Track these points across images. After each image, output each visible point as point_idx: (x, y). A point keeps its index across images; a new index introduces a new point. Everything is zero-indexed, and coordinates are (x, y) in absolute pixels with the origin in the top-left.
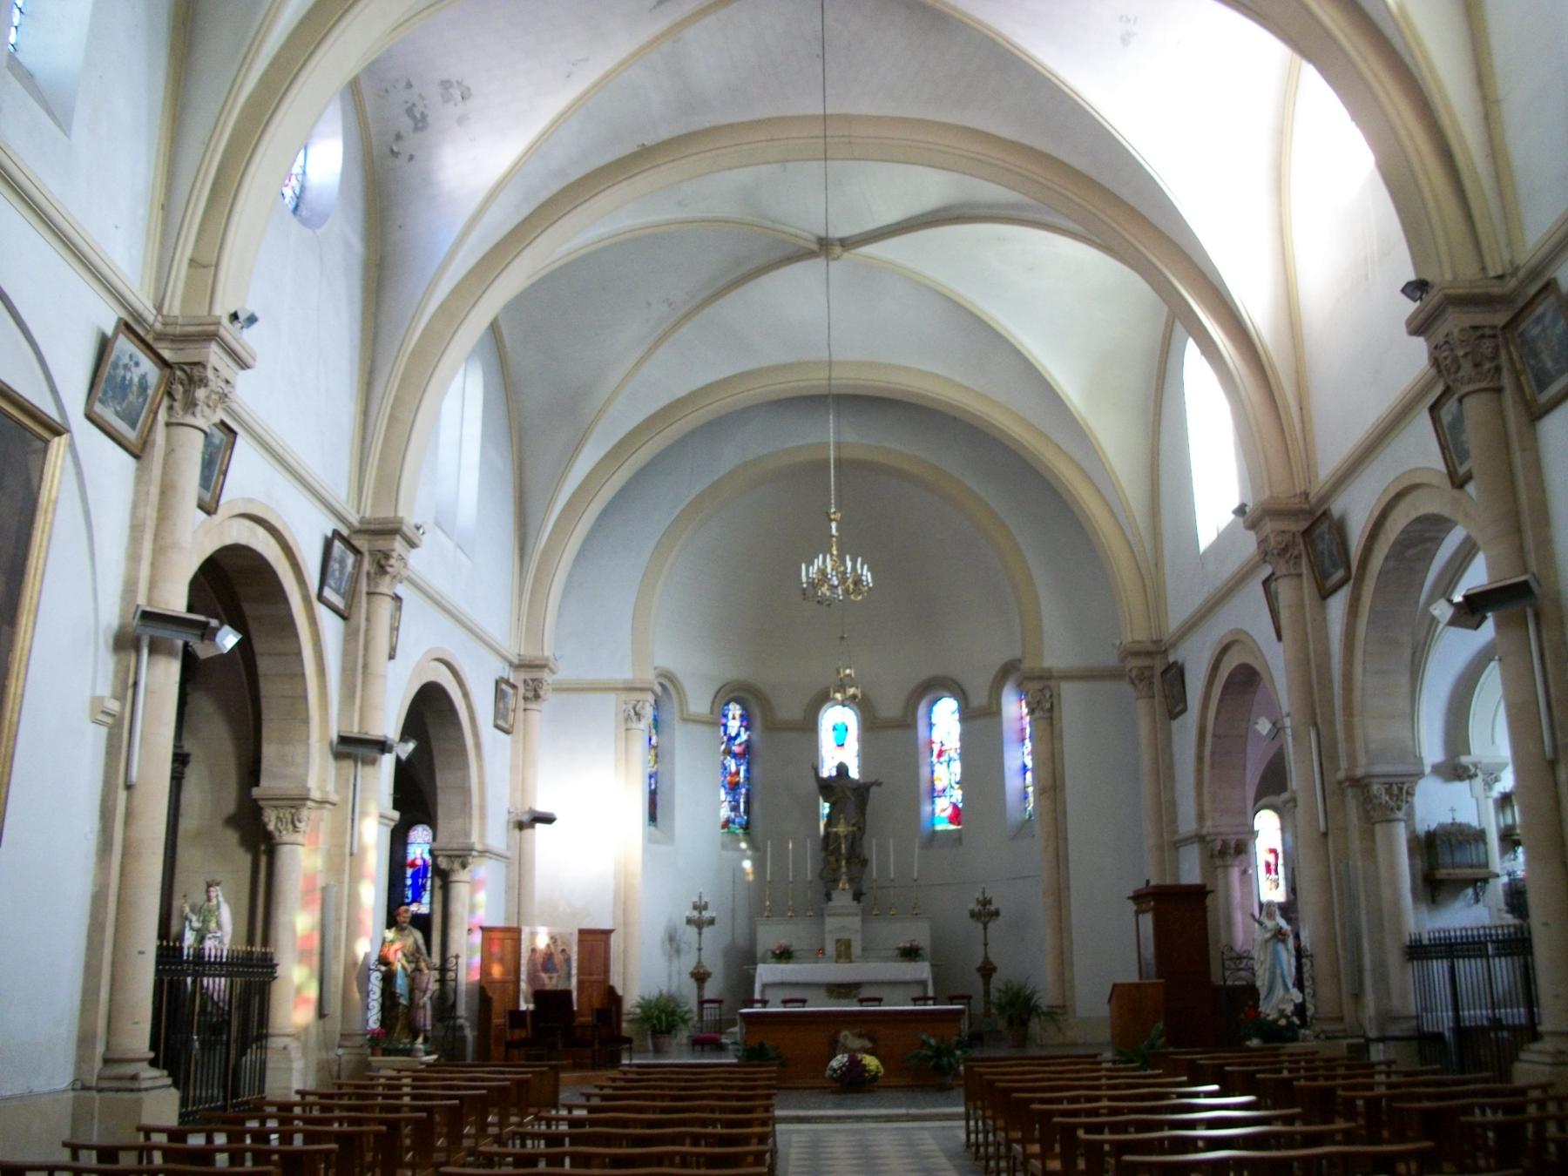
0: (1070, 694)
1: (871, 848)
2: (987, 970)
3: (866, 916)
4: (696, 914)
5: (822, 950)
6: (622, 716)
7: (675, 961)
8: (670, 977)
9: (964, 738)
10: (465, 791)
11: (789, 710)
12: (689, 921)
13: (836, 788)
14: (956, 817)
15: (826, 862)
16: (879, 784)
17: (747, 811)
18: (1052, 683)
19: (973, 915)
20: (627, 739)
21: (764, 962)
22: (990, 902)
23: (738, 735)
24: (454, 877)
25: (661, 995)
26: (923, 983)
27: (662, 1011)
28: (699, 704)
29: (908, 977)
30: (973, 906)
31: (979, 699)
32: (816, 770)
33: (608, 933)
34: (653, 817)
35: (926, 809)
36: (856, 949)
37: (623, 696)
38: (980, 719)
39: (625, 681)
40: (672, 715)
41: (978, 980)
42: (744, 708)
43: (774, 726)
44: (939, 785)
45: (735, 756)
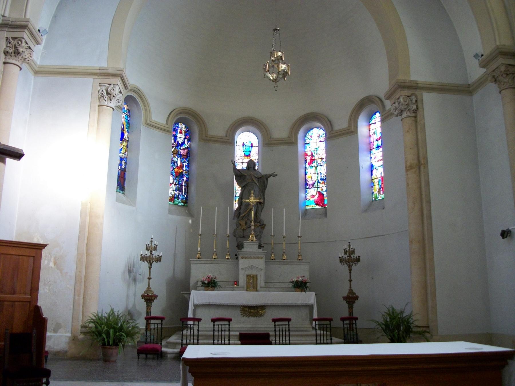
0: (428, 99)
1: (270, 216)
2: (351, 299)
3: (269, 260)
4: (148, 253)
5: (236, 283)
6: (96, 95)
7: (132, 287)
8: (128, 297)
9: (328, 150)
11: (217, 130)
12: (143, 258)
13: (248, 177)
14: (320, 200)
15: (238, 225)
16: (275, 176)
17: (187, 192)
18: (417, 92)
19: (341, 260)
20: (99, 112)
21: (196, 289)
22: (353, 252)
23: (183, 143)
25: (112, 313)
26: (310, 307)
27: (109, 326)
28: (159, 116)
29: (299, 303)
30: (342, 254)
31: (341, 124)
32: (234, 165)
33: (40, 247)
34: (121, 185)
35: (302, 195)
36: (261, 282)
37: (99, 80)
38: (343, 138)
40: (139, 120)
41: (345, 305)
42: (187, 127)
43: (206, 139)
44: (310, 182)
45: (180, 156)
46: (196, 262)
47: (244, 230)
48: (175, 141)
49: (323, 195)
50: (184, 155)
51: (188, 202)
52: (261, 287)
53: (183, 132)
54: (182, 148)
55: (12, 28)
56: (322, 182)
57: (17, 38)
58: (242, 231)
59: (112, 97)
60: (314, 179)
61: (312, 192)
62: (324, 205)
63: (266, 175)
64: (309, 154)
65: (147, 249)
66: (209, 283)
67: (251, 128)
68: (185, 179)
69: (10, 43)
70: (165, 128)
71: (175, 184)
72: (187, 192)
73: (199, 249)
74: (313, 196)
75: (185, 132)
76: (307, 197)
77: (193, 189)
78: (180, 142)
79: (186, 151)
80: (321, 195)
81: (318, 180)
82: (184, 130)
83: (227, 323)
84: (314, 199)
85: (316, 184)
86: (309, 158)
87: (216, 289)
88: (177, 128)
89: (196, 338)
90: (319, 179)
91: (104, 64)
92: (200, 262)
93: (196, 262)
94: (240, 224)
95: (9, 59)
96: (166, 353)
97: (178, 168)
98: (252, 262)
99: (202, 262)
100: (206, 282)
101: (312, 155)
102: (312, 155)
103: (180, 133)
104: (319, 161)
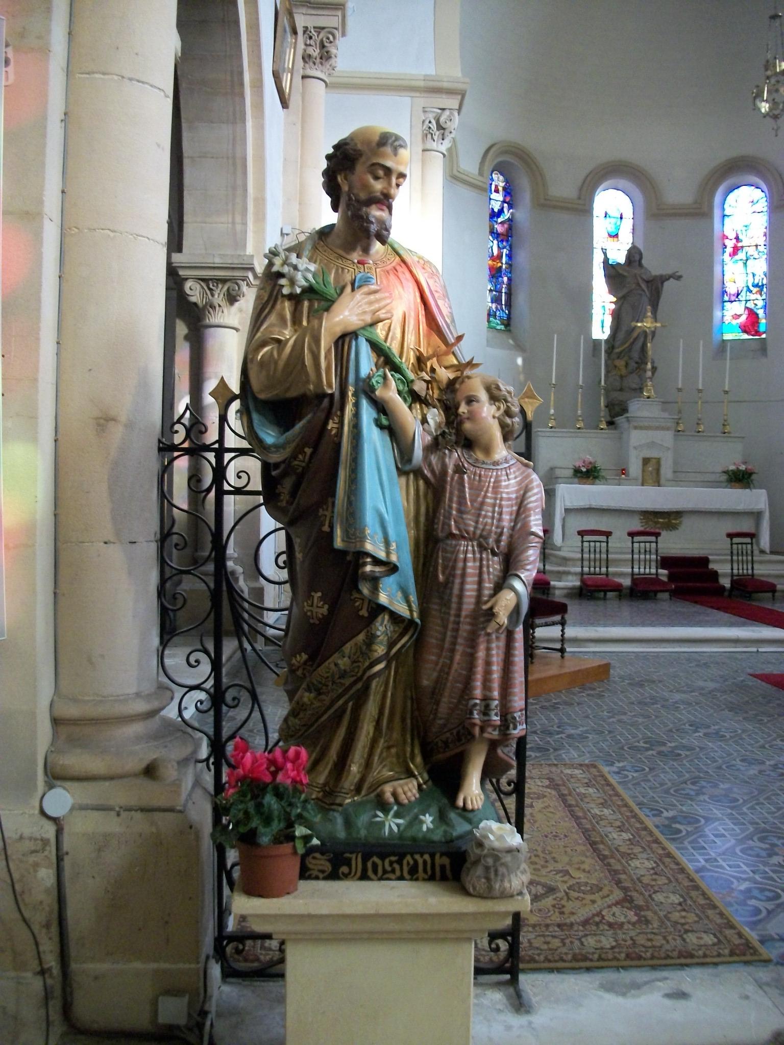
5: (624, 471)
10: (236, 164)
11: (563, 187)
14: (751, 323)
16: (679, 278)
17: (509, 304)
20: (423, 162)
23: (501, 211)
24: (214, 318)
29: (741, 507)
35: (717, 314)
36: (666, 471)
37: (422, 101)
39: (426, 78)
42: (507, 181)
43: (545, 204)
44: (731, 289)
46: (548, 434)
47: (622, 377)
49: (757, 315)
50: (502, 234)
51: (512, 323)
53: (500, 189)
54: (500, 220)
55: (314, 8)
56: (755, 290)
57: (323, 28)
58: (618, 378)
59: (447, 133)
60: (741, 284)
61: (737, 308)
62: (757, 333)
63: (661, 276)
64: (732, 235)
66: (588, 471)
67: (622, 183)
68: (505, 279)
69: (311, 38)
70: (480, 184)
72: (509, 304)
73: (552, 411)
74: (737, 317)
75: (504, 189)
76: (725, 318)
77: (521, 299)
78: (496, 210)
80: (752, 315)
81: (748, 287)
82: (501, 185)
83: (603, 538)
85: (743, 294)
86: (730, 244)
87: (597, 481)
89: (604, 563)
91: (429, 70)
92: (552, 434)
93: (548, 434)
94: (616, 366)
95: (310, 68)
96: (555, 588)
98: (647, 432)
99: (560, 435)
100: (584, 470)
102: (737, 238)
104: (752, 251)
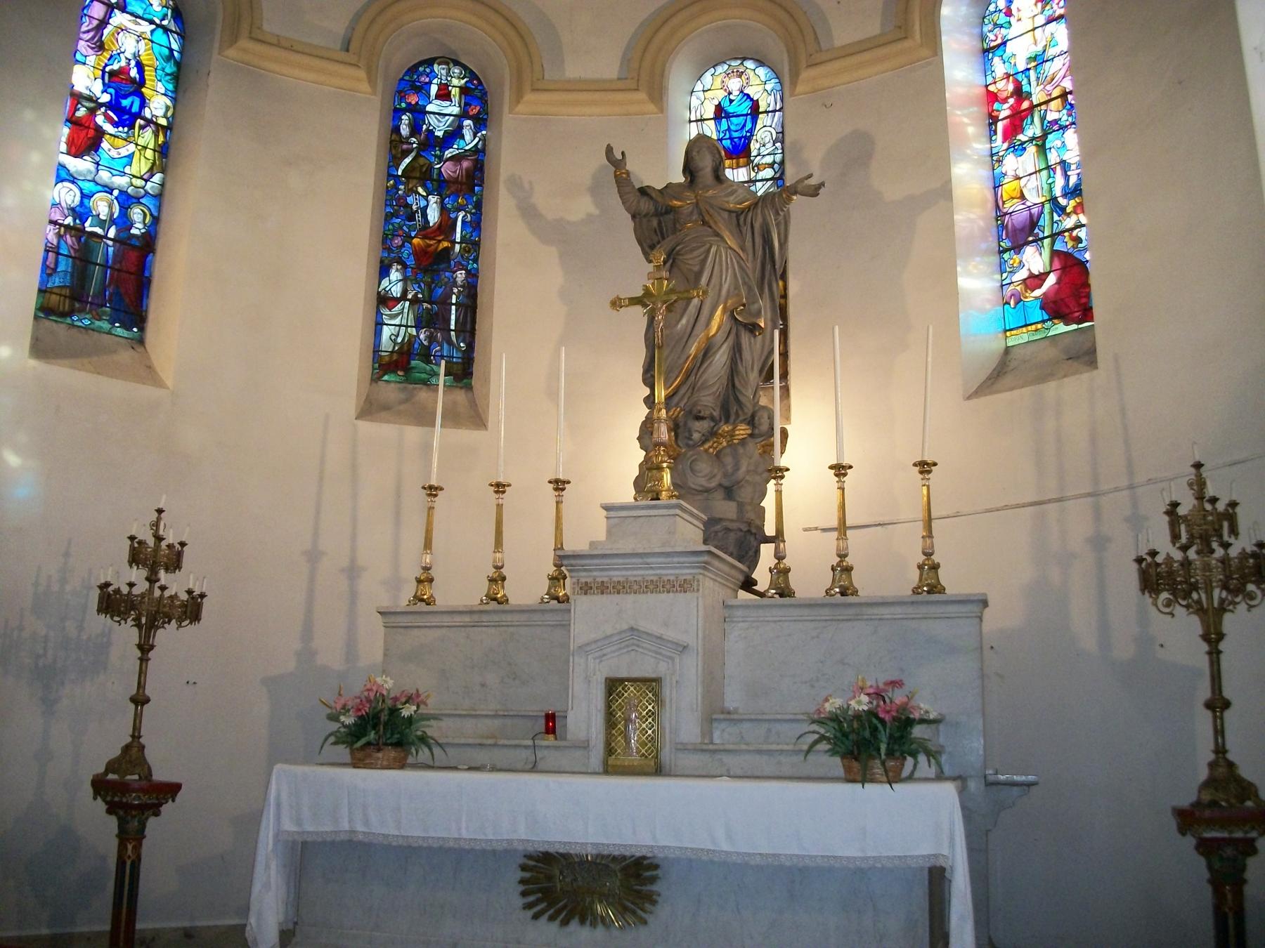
5: (551, 723)
12: (112, 603)
23: (455, 134)
36: (682, 717)
45: (441, 186)
48: (415, 128)
52: (683, 748)
53: (455, 92)
54: (448, 154)
65: (136, 558)
68: (460, 276)
71: (414, 301)
74: (1035, 280)
75: (464, 90)
78: (439, 134)
79: (465, 164)
81: (1053, 200)
84: (1038, 293)
85: (1045, 221)
86: (1004, 111)
88: (424, 79)
90: (1058, 192)
97: (425, 229)
101: (1019, 93)
102: (1019, 93)
103: (438, 97)
104: (1054, 112)
